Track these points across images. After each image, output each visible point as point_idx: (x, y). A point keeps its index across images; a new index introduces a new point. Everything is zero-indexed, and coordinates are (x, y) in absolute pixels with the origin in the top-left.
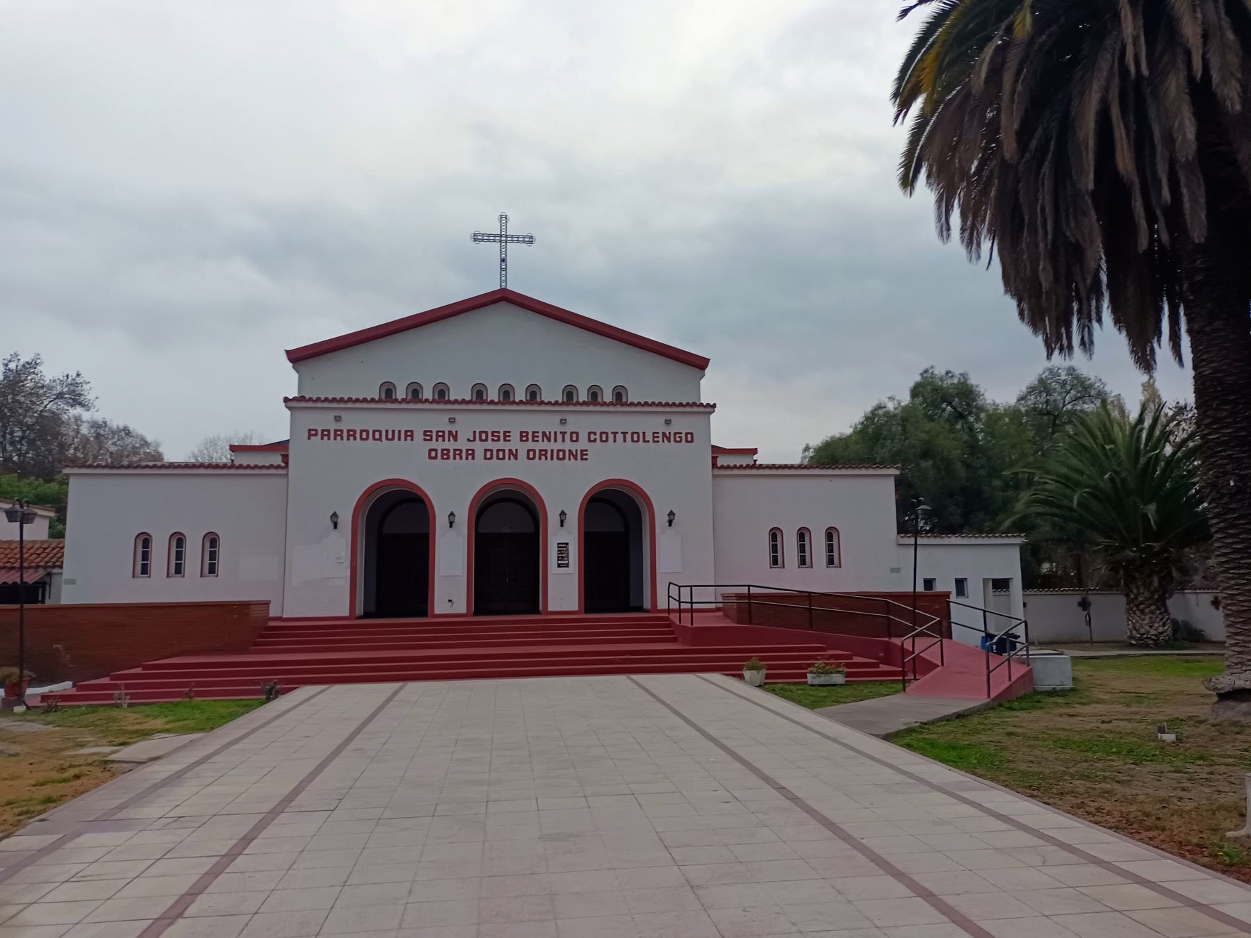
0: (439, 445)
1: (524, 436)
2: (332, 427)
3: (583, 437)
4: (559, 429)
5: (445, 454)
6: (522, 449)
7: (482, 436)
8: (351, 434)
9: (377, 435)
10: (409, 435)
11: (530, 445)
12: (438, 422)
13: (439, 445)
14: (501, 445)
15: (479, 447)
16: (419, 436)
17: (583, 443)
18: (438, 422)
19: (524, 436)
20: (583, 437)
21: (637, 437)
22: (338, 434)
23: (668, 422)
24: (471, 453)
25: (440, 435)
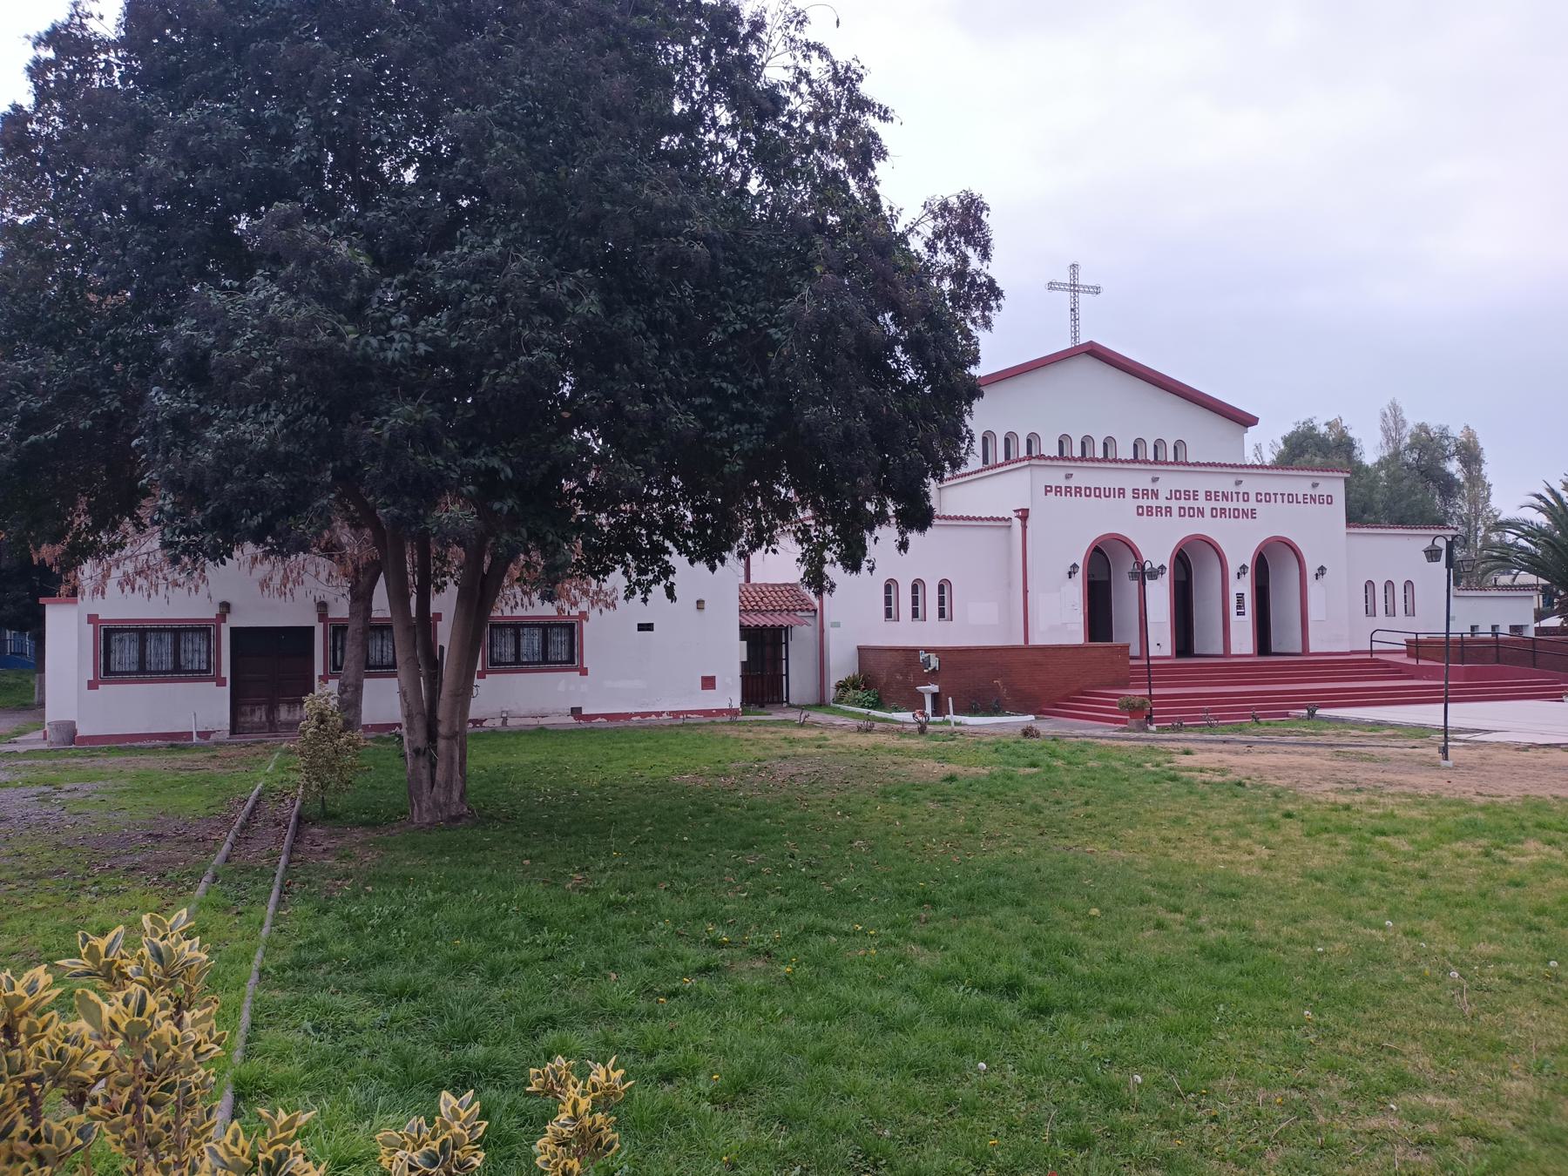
0: (1145, 502)
1: (1208, 494)
2: (1063, 483)
3: (1252, 497)
4: (1234, 489)
5: (1150, 510)
6: (1207, 506)
7: (1175, 494)
8: (1078, 490)
9: (1098, 492)
10: (1122, 492)
11: (1213, 504)
12: (1143, 481)
13: (1145, 502)
14: (1191, 503)
15: (1175, 505)
16: (1129, 493)
17: (1252, 504)
18: (1143, 481)
19: (1208, 494)
20: (1252, 497)
21: (1291, 498)
22: (1068, 490)
23: (1315, 485)
24: (1169, 510)
25: (1145, 493)
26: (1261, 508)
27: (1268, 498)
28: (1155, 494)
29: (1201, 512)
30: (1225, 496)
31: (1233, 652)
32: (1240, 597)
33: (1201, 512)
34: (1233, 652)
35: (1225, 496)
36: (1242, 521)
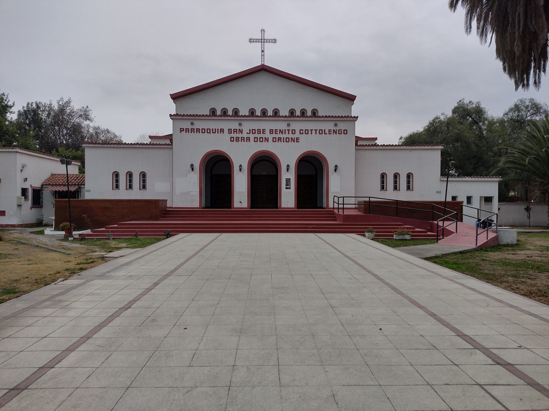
0: (235, 135)
2: (190, 127)
3: (297, 132)
4: (287, 128)
7: (253, 131)
8: (198, 130)
9: (209, 131)
10: (222, 131)
11: (274, 135)
13: (235, 135)
14: (261, 135)
15: (252, 136)
16: (226, 131)
18: (234, 125)
20: (297, 132)
22: (192, 130)
24: (248, 139)
25: (235, 131)
26: (302, 137)
27: (307, 132)
28: (241, 131)
29: (267, 140)
30: (281, 132)
31: (282, 207)
32: (288, 181)
33: (267, 140)
34: (282, 207)
35: (281, 132)
36: (291, 144)
